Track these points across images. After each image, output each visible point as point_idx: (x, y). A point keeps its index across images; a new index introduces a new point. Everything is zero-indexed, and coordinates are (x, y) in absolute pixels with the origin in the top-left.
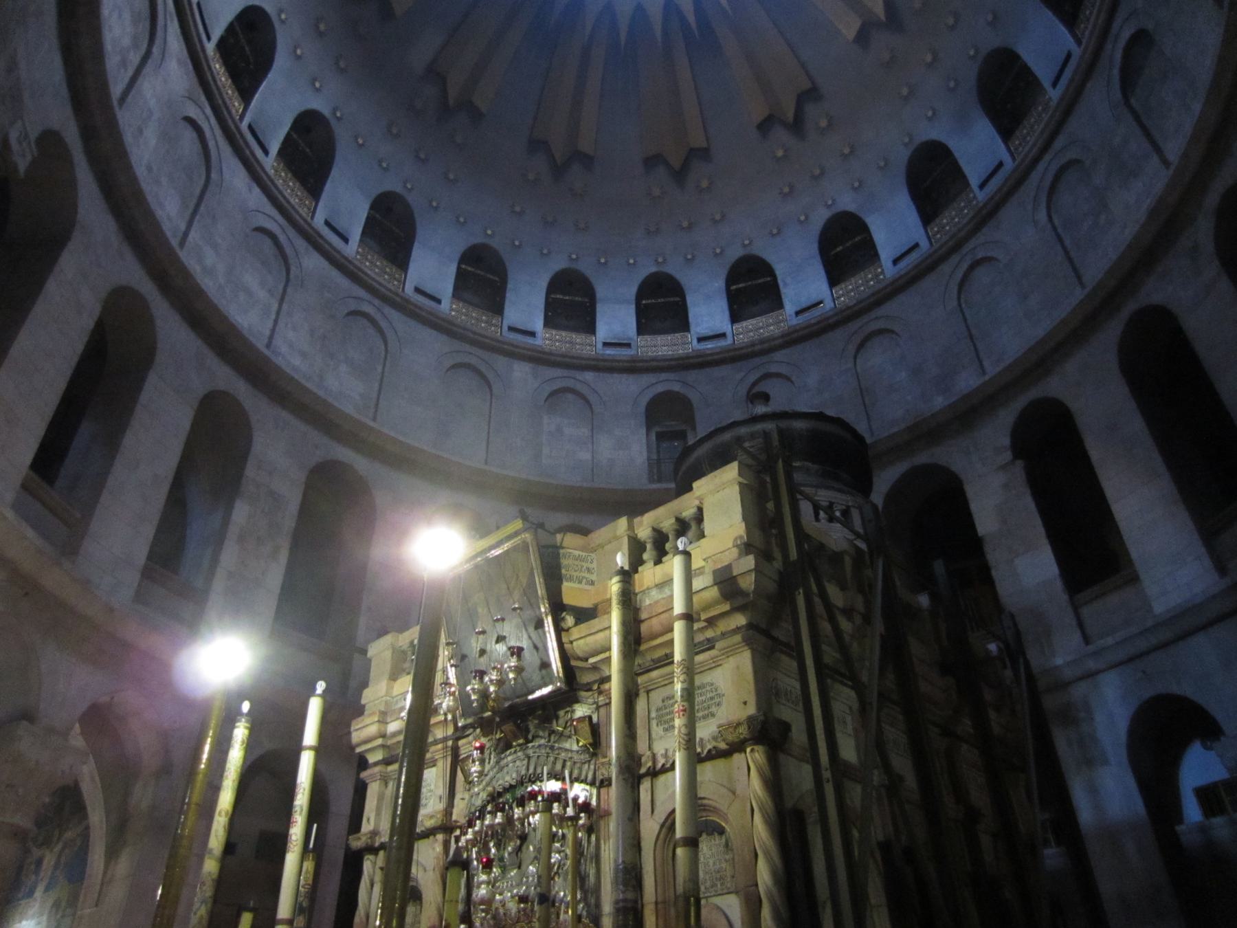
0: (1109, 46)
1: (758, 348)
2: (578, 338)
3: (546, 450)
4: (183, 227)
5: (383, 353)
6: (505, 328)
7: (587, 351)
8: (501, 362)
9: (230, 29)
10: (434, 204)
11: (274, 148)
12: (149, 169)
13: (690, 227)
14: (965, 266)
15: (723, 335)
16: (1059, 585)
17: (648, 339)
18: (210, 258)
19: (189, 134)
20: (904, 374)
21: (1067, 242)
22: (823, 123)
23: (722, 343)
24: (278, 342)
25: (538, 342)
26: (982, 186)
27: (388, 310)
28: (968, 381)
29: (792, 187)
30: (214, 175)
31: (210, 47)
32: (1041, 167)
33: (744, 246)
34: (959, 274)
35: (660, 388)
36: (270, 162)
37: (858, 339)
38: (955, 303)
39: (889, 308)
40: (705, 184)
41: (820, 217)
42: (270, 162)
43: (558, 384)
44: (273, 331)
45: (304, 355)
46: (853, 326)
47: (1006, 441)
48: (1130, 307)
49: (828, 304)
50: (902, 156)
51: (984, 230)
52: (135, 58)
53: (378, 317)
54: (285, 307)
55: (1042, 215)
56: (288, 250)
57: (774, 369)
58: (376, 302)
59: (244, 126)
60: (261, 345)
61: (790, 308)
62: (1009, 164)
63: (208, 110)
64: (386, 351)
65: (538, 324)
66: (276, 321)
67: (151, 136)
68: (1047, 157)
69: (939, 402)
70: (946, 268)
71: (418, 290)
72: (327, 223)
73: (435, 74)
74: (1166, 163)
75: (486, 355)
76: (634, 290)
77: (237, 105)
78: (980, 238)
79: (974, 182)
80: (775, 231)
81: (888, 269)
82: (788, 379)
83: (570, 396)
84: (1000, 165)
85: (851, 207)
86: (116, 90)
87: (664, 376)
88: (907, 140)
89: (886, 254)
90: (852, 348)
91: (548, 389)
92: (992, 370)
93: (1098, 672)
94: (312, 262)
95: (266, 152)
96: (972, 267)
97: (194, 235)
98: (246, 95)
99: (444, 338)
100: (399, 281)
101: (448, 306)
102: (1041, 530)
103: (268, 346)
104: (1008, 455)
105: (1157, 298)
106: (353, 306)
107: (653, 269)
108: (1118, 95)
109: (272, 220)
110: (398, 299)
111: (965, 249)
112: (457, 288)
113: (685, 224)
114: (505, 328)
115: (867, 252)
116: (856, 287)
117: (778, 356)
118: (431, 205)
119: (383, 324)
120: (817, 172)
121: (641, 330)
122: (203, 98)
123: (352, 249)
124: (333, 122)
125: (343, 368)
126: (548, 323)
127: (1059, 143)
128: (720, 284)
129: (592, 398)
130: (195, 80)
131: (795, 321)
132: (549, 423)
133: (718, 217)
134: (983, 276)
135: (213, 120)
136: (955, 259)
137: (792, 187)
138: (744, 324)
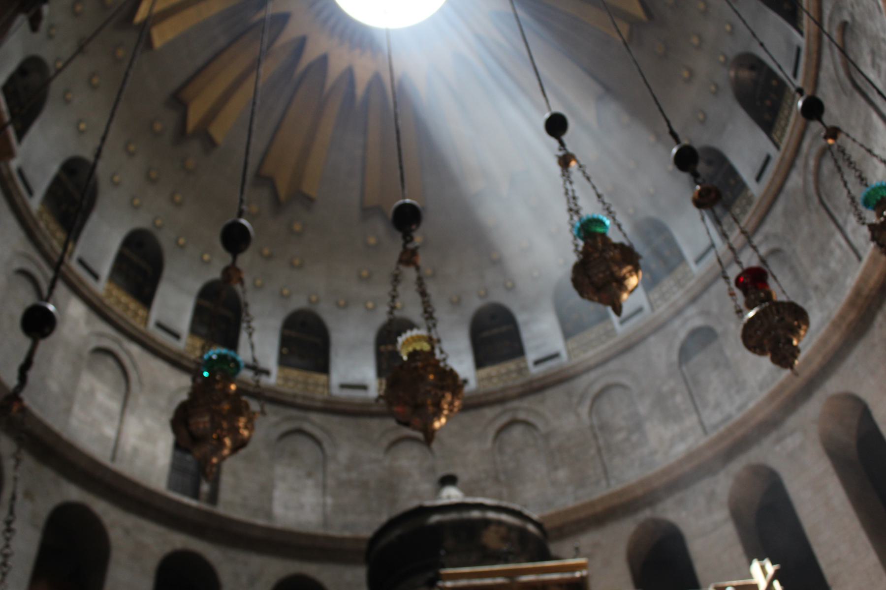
1: (299, 401)
3: (76, 409)
13: (270, 257)
14: (505, 419)
21: (601, 442)
32: (592, 375)
33: (310, 301)
43: (106, 343)
55: (584, 410)
57: (307, 427)
65: (105, 269)
68: (600, 371)
70: (489, 413)
78: (525, 403)
80: (342, 302)
82: (318, 442)
83: (110, 361)
88: (482, 292)
90: (385, 442)
91: (94, 343)
96: (513, 422)
101: (35, 204)
113: (266, 251)
117: (316, 417)
127: (612, 365)
129: (133, 375)
131: (336, 392)
132: (87, 381)
133: (297, 262)
134: (517, 432)
136: (497, 409)
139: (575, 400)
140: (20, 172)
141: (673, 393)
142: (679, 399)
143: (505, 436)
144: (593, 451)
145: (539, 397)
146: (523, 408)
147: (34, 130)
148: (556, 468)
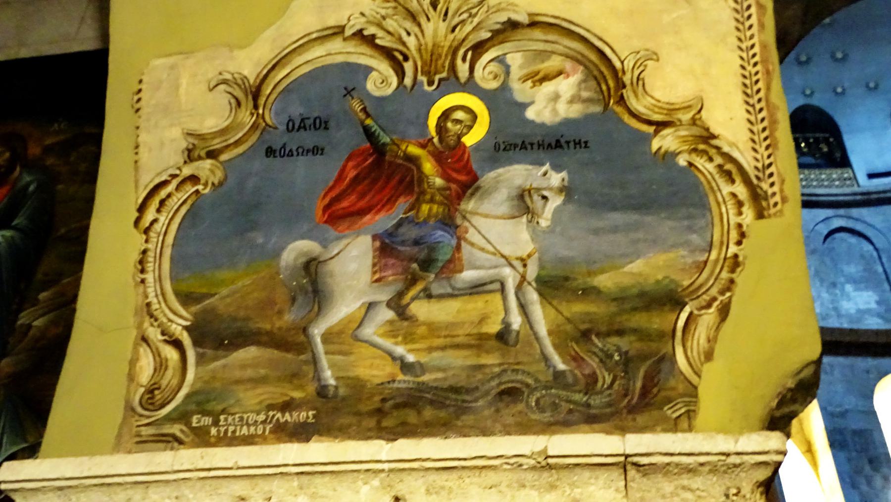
5: (875, 254)
10: (839, 90)
27: (855, 212)
58: (842, 211)
64: (876, 249)
71: (871, 176)
100: (850, 179)
106: (824, 229)
110: (859, 197)
118: (837, 93)
119: (859, 227)
125: (849, 288)
147: (850, 142)
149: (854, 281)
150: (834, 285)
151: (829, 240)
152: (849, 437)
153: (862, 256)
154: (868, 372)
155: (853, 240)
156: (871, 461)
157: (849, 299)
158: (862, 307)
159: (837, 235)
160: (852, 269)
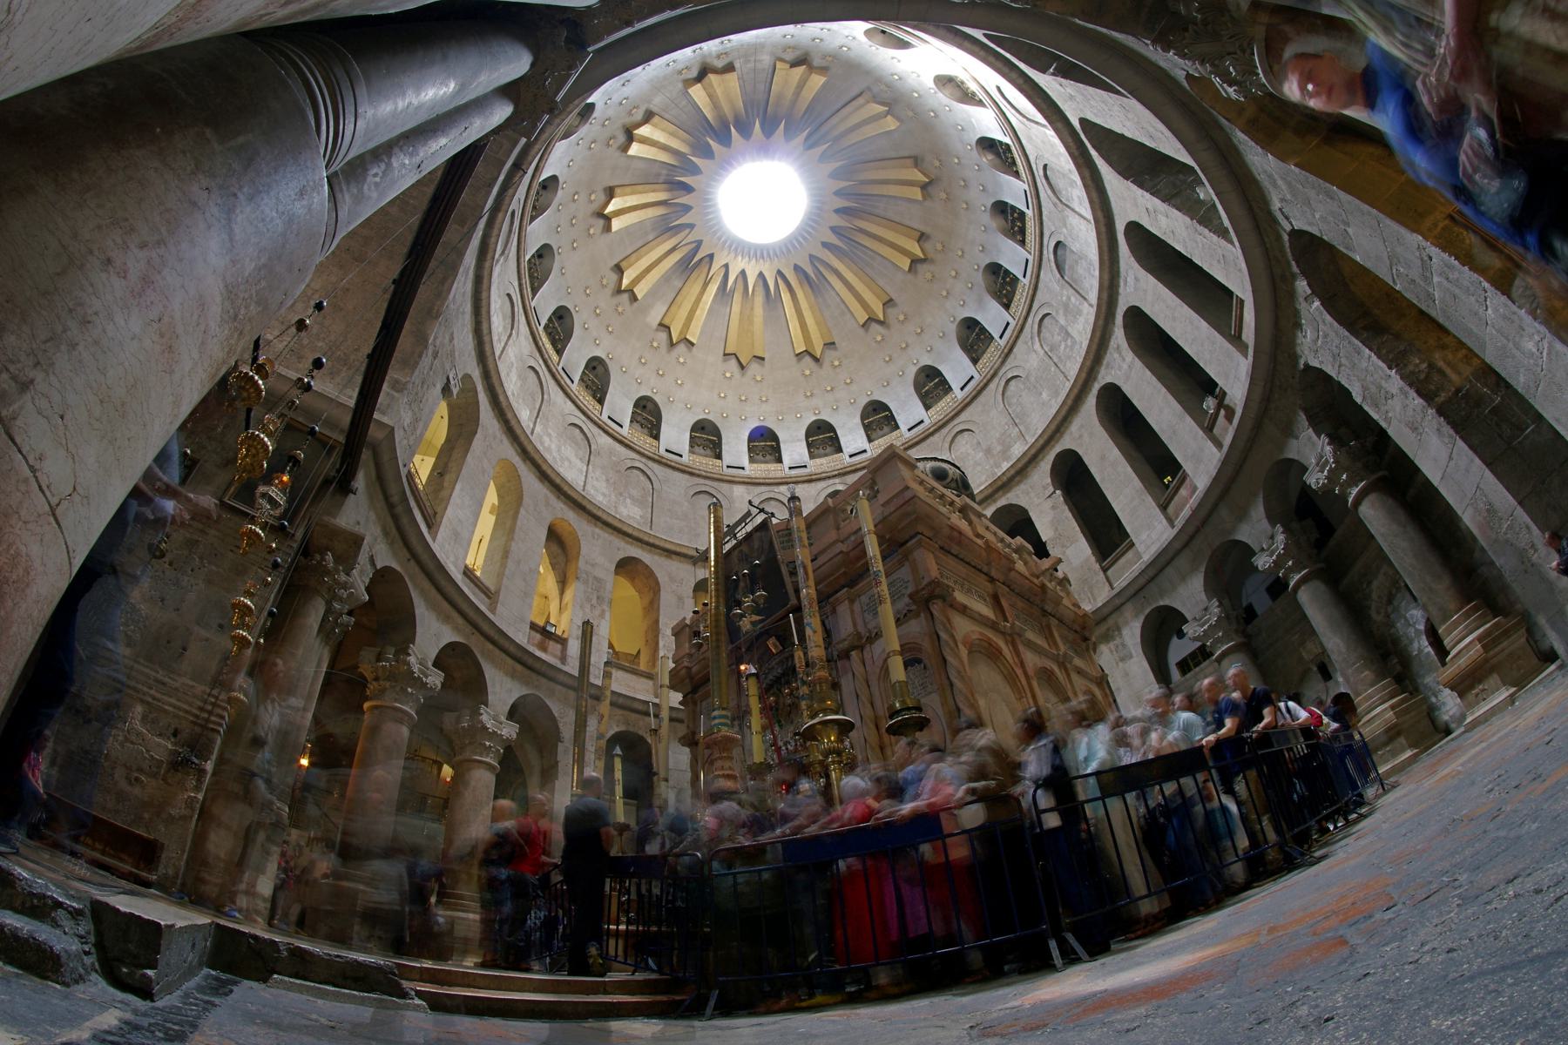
0: (1045, 252)
2: (773, 466)
4: (532, 426)
6: (725, 467)
7: (779, 474)
8: (725, 486)
9: (550, 320)
11: (577, 379)
12: (513, 395)
14: (1003, 383)
15: (865, 451)
16: (1093, 559)
17: (818, 461)
18: (546, 439)
19: (532, 374)
20: (981, 454)
22: (901, 317)
23: (863, 456)
24: (588, 487)
25: (747, 472)
26: (1001, 337)
27: (650, 464)
28: (1018, 450)
29: (890, 357)
30: (545, 397)
31: (541, 329)
34: (1001, 389)
35: (830, 490)
36: (575, 387)
37: (950, 439)
38: (1002, 406)
39: (963, 416)
40: (836, 363)
41: (912, 371)
42: (575, 387)
44: (585, 482)
45: (604, 495)
46: (944, 431)
47: (1049, 480)
48: (1096, 387)
49: (927, 422)
50: (952, 329)
51: (1009, 360)
52: (504, 338)
53: (645, 469)
54: (590, 467)
55: (1037, 346)
56: (589, 435)
58: (644, 460)
59: (560, 368)
60: (580, 489)
61: (903, 428)
62: (1013, 323)
63: (541, 362)
65: (745, 462)
66: (586, 476)
67: (514, 377)
68: (1032, 315)
69: (1005, 466)
70: (992, 386)
72: (609, 417)
73: (664, 326)
74: (1091, 305)
75: (715, 484)
76: (804, 432)
77: (555, 357)
79: (996, 336)
81: (958, 394)
84: (1008, 324)
85: (929, 363)
86: (497, 354)
87: (831, 481)
89: (955, 385)
90: (947, 445)
92: (1031, 440)
93: (1123, 604)
94: (604, 440)
95: (573, 382)
97: (538, 429)
98: (560, 352)
99: (687, 477)
102: (1078, 528)
103: (584, 490)
104: (1051, 489)
105: (1109, 380)
107: (814, 418)
108: (1058, 275)
109: (580, 419)
111: (1000, 373)
112: (691, 446)
113: (829, 388)
114: (725, 467)
115: (945, 387)
116: (943, 406)
119: (649, 473)
120: (904, 346)
121: (812, 456)
122: (538, 355)
123: (625, 431)
124: (607, 361)
125: (628, 501)
126: (752, 460)
128: (858, 420)
130: (534, 346)
131: (908, 435)
133: (848, 381)
135: (543, 367)
136: (996, 380)
137: (890, 357)
138: (876, 442)
139: (1030, 343)
140: (667, 450)
141: (1069, 298)
142: (1073, 299)
143: (1008, 393)
144: (1053, 369)
145: (1012, 356)
146: (1008, 371)
148: (1041, 394)
149: (632, 498)
150: (621, 494)
151: (629, 471)
152: (591, 580)
153: (644, 489)
154: (619, 549)
155: (642, 478)
156: (598, 598)
157: (626, 507)
158: (632, 515)
159: (634, 471)
160: (634, 492)
